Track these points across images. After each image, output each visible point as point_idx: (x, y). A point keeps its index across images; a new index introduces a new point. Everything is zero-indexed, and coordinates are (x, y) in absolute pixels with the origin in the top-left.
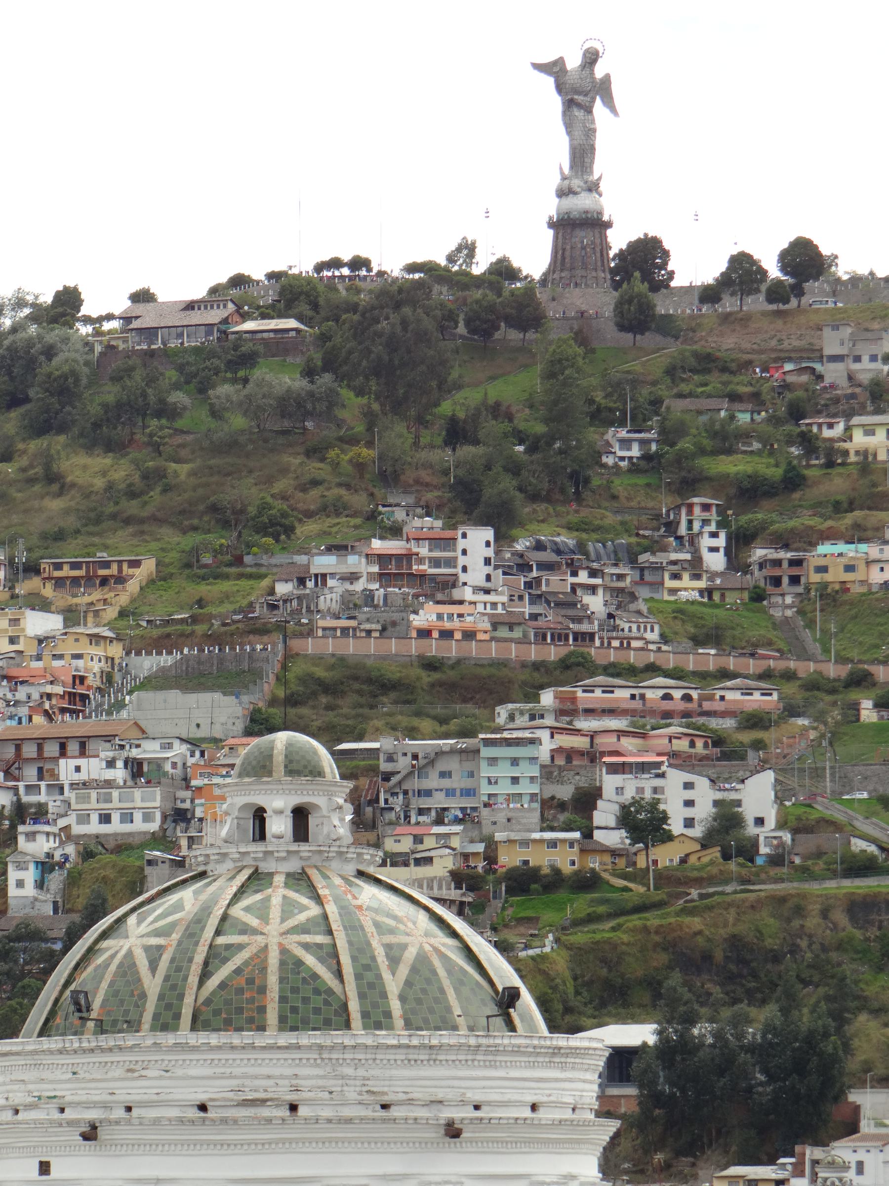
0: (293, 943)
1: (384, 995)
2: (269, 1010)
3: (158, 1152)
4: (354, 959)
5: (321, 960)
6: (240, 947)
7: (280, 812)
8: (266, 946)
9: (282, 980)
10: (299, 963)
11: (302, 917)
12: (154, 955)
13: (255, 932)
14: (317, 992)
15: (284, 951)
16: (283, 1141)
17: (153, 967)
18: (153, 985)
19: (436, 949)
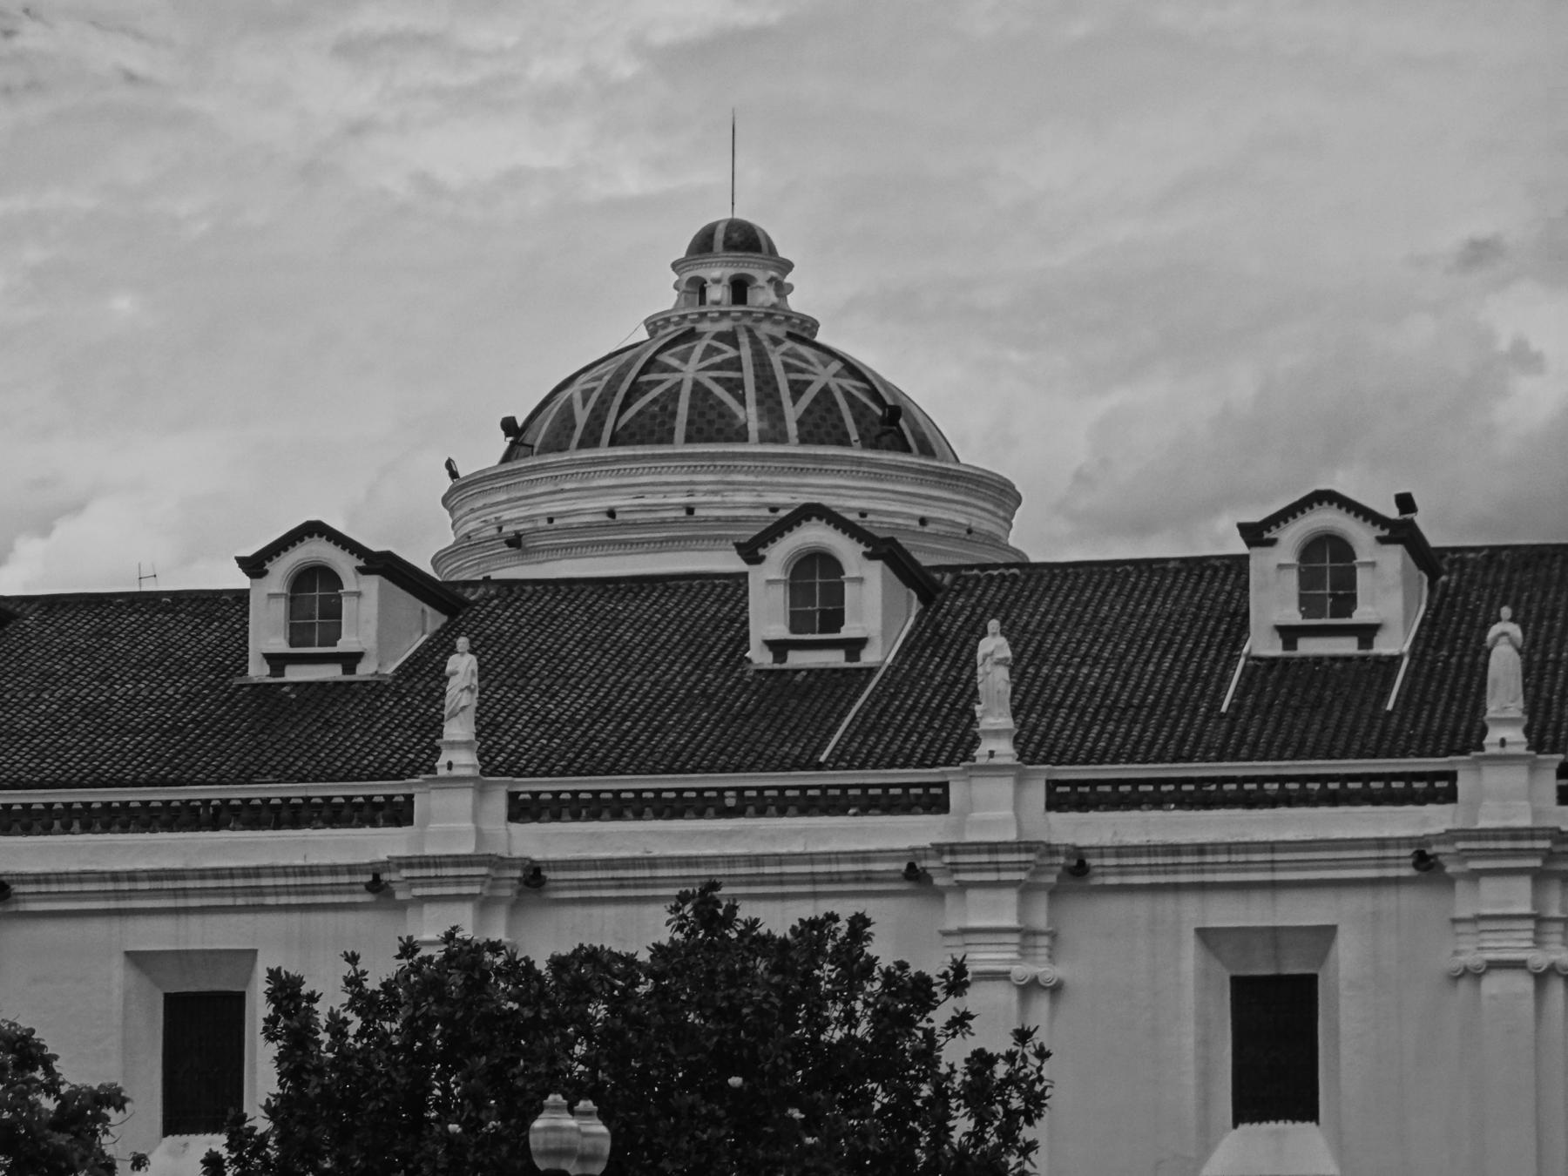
0: (706, 379)
1: (782, 418)
2: (677, 431)
3: (573, 555)
4: (758, 389)
5: (729, 390)
6: (660, 382)
7: (717, 281)
8: (682, 381)
9: (691, 407)
10: (708, 392)
11: (718, 359)
12: (586, 395)
13: (675, 370)
14: (721, 416)
15: (697, 384)
16: (679, 539)
17: (584, 405)
18: (582, 416)
19: (841, 387)
